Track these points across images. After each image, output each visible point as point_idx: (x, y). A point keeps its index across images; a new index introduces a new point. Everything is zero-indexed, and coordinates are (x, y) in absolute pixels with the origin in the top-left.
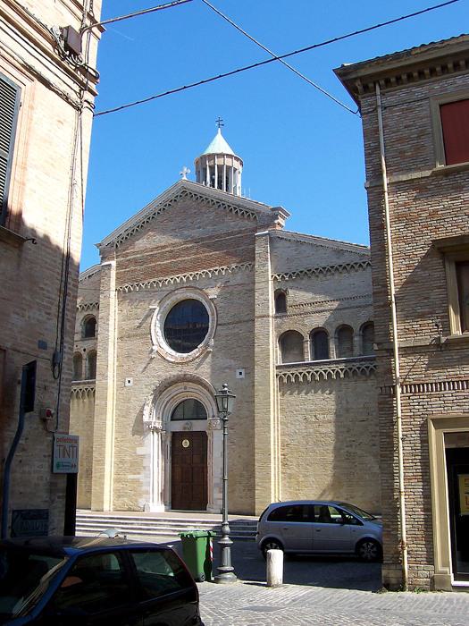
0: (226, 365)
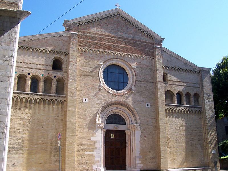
0: (141, 100)
